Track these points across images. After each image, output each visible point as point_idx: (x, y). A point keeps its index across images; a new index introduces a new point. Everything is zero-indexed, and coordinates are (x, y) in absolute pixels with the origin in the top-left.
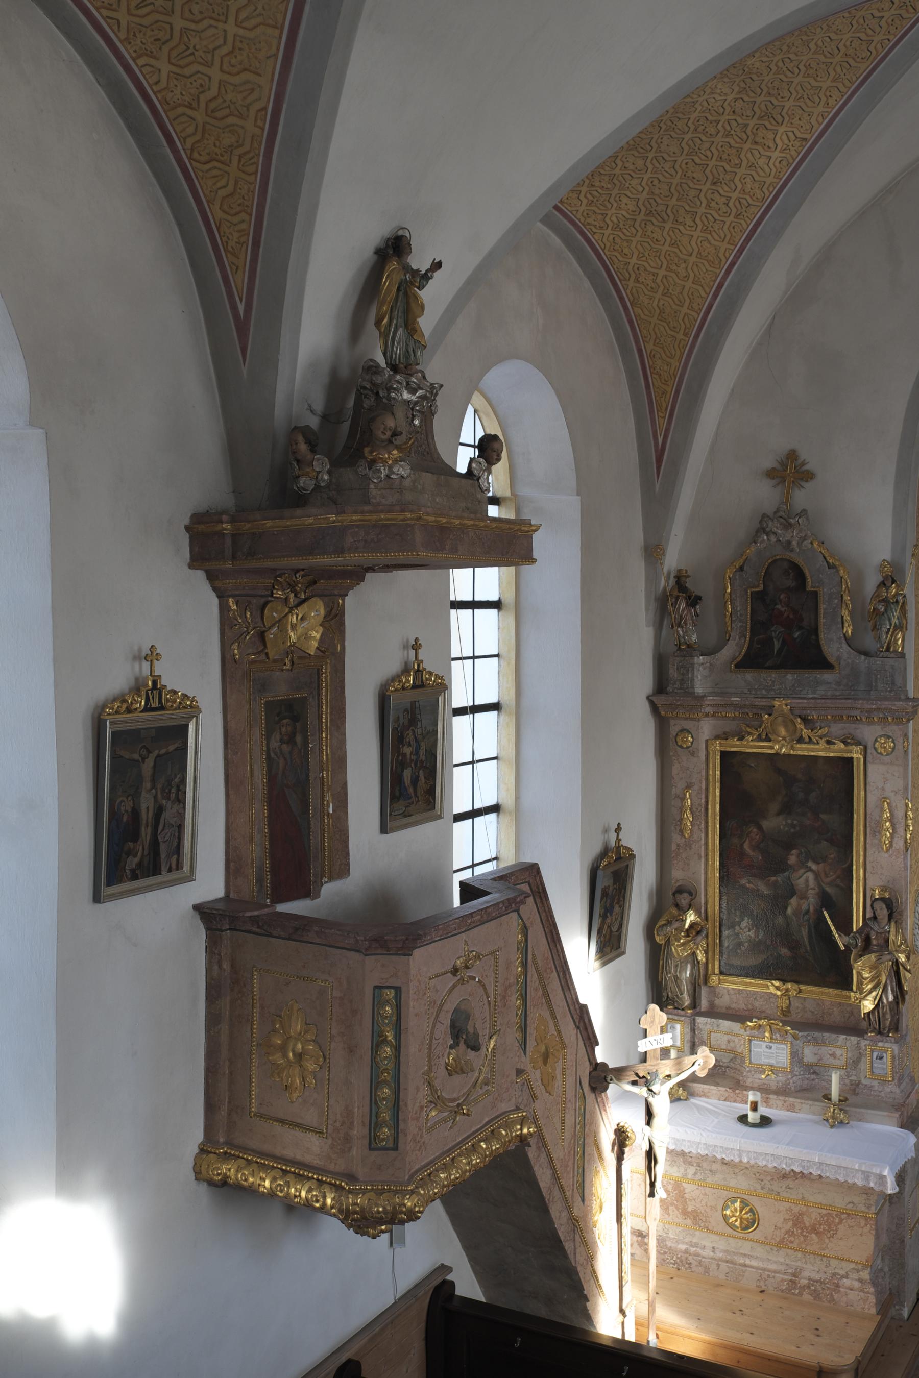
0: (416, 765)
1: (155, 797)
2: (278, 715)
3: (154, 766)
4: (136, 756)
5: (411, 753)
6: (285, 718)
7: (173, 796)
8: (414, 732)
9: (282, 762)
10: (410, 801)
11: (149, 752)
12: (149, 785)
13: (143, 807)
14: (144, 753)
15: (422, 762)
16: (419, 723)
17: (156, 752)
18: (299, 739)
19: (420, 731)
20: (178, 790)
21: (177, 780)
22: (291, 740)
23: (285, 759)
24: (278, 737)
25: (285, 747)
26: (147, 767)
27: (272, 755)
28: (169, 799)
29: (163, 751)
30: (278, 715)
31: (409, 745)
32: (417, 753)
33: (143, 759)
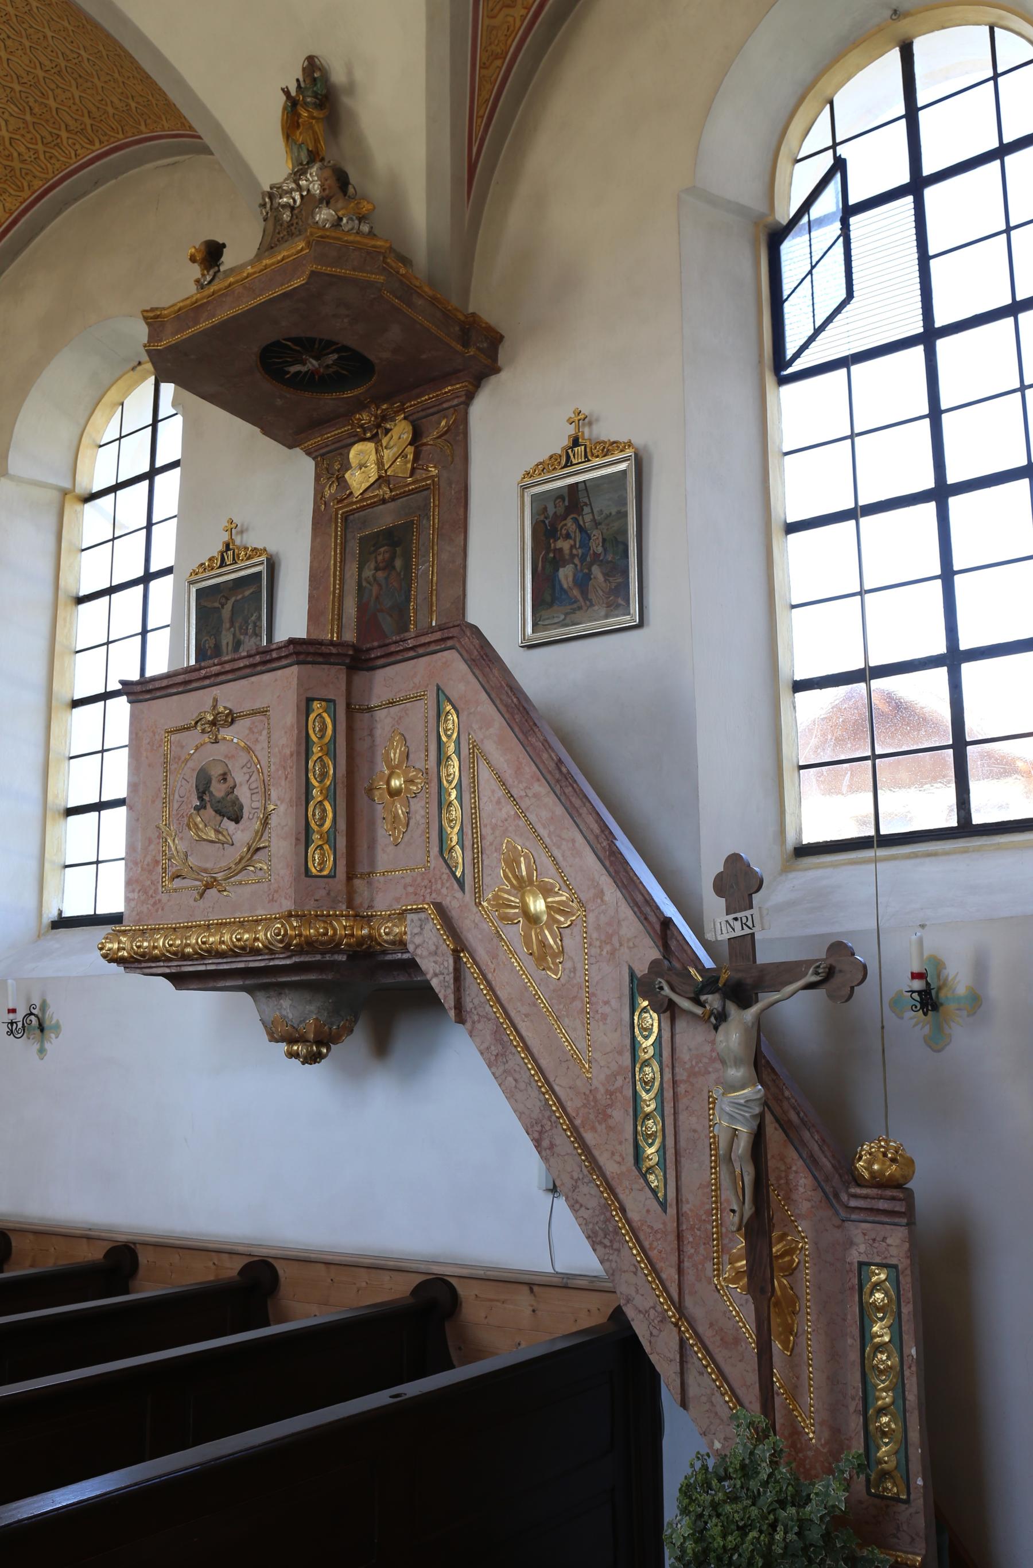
0: (583, 559)
1: (234, 635)
2: (374, 545)
3: (232, 610)
4: (217, 605)
5: (572, 547)
6: (383, 546)
7: (250, 631)
8: (576, 520)
9: (375, 589)
10: (575, 606)
11: (227, 599)
12: (228, 625)
13: (224, 643)
14: (223, 600)
15: (596, 555)
16: (587, 510)
17: (233, 599)
18: (398, 563)
19: (588, 518)
20: (255, 626)
21: (253, 618)
22: (388, 566)
23: (380, 585)
24: (372, 565)
25: (380, 574)
26: (226, 612)
27: (364, 584)
28: (246, 634)
29: (239, 597)
30: (374, 545)
31: (568, 536)
32: (585, 545)
33: (223, 606)
